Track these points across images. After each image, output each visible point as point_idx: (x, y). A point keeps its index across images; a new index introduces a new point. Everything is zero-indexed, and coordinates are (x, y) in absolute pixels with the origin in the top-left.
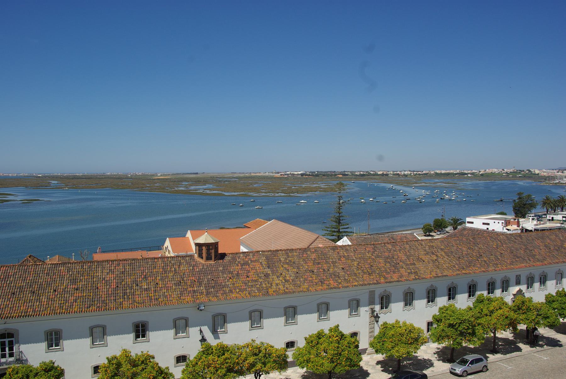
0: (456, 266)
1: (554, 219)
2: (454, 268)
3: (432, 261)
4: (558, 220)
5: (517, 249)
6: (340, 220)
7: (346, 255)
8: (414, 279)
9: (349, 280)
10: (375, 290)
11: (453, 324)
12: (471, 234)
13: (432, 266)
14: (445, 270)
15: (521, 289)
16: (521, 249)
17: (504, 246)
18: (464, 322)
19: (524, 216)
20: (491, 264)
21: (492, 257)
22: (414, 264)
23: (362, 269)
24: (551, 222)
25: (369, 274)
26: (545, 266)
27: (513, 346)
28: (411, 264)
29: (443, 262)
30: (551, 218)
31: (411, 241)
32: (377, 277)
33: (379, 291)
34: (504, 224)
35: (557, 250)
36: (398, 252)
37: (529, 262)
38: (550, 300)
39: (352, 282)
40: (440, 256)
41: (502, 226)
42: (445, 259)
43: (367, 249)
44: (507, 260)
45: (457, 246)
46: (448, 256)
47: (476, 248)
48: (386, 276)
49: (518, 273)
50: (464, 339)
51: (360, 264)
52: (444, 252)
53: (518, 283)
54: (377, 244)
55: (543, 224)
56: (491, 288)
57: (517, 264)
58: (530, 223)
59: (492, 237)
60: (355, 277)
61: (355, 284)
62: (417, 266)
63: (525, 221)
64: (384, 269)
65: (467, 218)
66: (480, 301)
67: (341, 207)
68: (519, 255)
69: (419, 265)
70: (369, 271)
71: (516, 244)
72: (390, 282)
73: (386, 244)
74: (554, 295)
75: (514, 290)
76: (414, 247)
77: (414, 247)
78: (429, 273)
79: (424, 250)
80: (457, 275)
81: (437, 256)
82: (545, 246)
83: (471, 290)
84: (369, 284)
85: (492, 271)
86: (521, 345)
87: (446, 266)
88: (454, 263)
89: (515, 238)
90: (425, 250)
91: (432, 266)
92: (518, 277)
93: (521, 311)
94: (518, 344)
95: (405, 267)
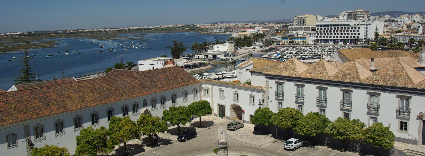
0: (97, 98)
1: (200, 57)
2: (96, 101)
3: (79, 97)
4: (202, 58)
5: (145, 82)
6: (28, 71)
7: (5, 100)
8: (61, 112)
9: (5, 120)
10: (29, 125)
11: (88, 141)
12: (119, 74)
13: (78, 101)
14: (88, 102)
15: (147, 109)
16: (148, 81)
17: (136, 80)
18: (96, 138)
19: (178, 57)
20: (124, 94)
21: (126, 90)
22: (64, 101)
23: (19, 109)
24: (198, 59)
25: (24, 113)
26: (164, 92)
27: (140, 149)
28: (61, 101)
29: (87, 96)
30: (197, 57)
31: (64, 84)
32: (31, 114)
33: (32, 125)
34: (164, 64)
35: (173, 80)
36: (52, 93)
37: (152, 90)
38: (166, 113)
39: (9, 121)
40: (86, 92)
41: (163, 65)
42: (89, 94)
43: (25, 93)
44: (137, 90)
45: (100, 84)
46: (92, 92)
47: (115, 84)
48: (39, 113)
49: (144, 99)
50: (98, 150)
51: (17, 106)
52: (89, 89)
53: (145, 105)
54: (34, 89)
55: (190, 61)
56: (125, 110)
57: (143, 93)
58: (182, 61)
59: (128, 75)
60: (11, 117)
61: (10, 122)
62: (66, 102)
63: (178, 60)
64: (38, 107)
65: (139, 61)
66: (112, 122)
67: (28, 61)
68: (146, 86)
69: (69, 102)
70: (24, 110)
71: (145, 78)
72: (41, 117)
73: (42, 88)
74: (168, 110)
75: (142, 110)
76: (66, 88)
77: (66, 88)
78: (75, 106)
79: (74, 89)
80: (97, 105)
81: (83, 93)
82: (165, 78)
83: (110, 114)
84: (23, 121)
85: (124, 99)
86: (146, 148)
87: (90, 100)
88: (96, 97)
89: (145, 75)
90: (74, 90)
91: (78, 101)
92: (145, 101)
93: (143, 124)
94: (144, 147)
95: (56, 104)
